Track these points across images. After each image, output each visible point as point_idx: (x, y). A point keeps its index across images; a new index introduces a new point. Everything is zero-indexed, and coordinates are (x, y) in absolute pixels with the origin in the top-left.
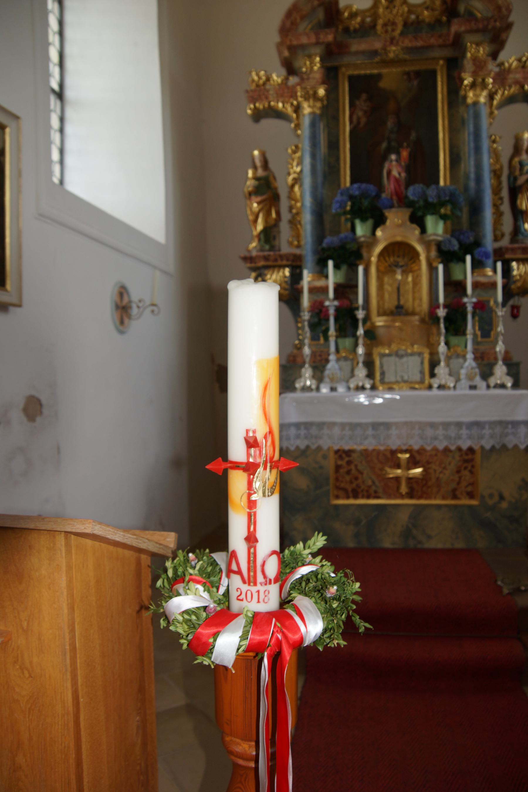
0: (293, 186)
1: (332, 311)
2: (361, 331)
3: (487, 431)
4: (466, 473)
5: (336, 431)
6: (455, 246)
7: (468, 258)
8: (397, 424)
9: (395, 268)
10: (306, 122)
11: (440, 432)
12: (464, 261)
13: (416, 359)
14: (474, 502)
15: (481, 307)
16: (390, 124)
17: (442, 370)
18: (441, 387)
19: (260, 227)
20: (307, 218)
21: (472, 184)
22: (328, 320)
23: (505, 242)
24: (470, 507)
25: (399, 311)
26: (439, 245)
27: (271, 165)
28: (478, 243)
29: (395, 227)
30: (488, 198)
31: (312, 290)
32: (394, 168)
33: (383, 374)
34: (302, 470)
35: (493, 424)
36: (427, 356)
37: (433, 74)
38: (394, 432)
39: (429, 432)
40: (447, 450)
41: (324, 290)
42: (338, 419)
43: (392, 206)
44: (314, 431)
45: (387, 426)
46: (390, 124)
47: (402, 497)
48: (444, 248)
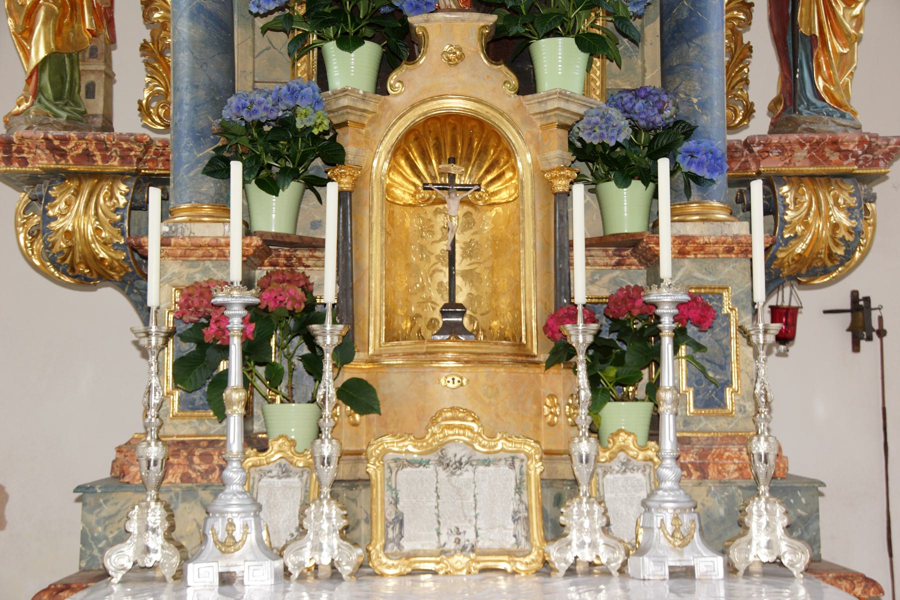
2: (329, 386)
7: (664, 165)
9: (444, 194)
12: (649, 177)
15: (698, 312)
19: (39, 51)
22: (224, 351)
28: (683, 129)
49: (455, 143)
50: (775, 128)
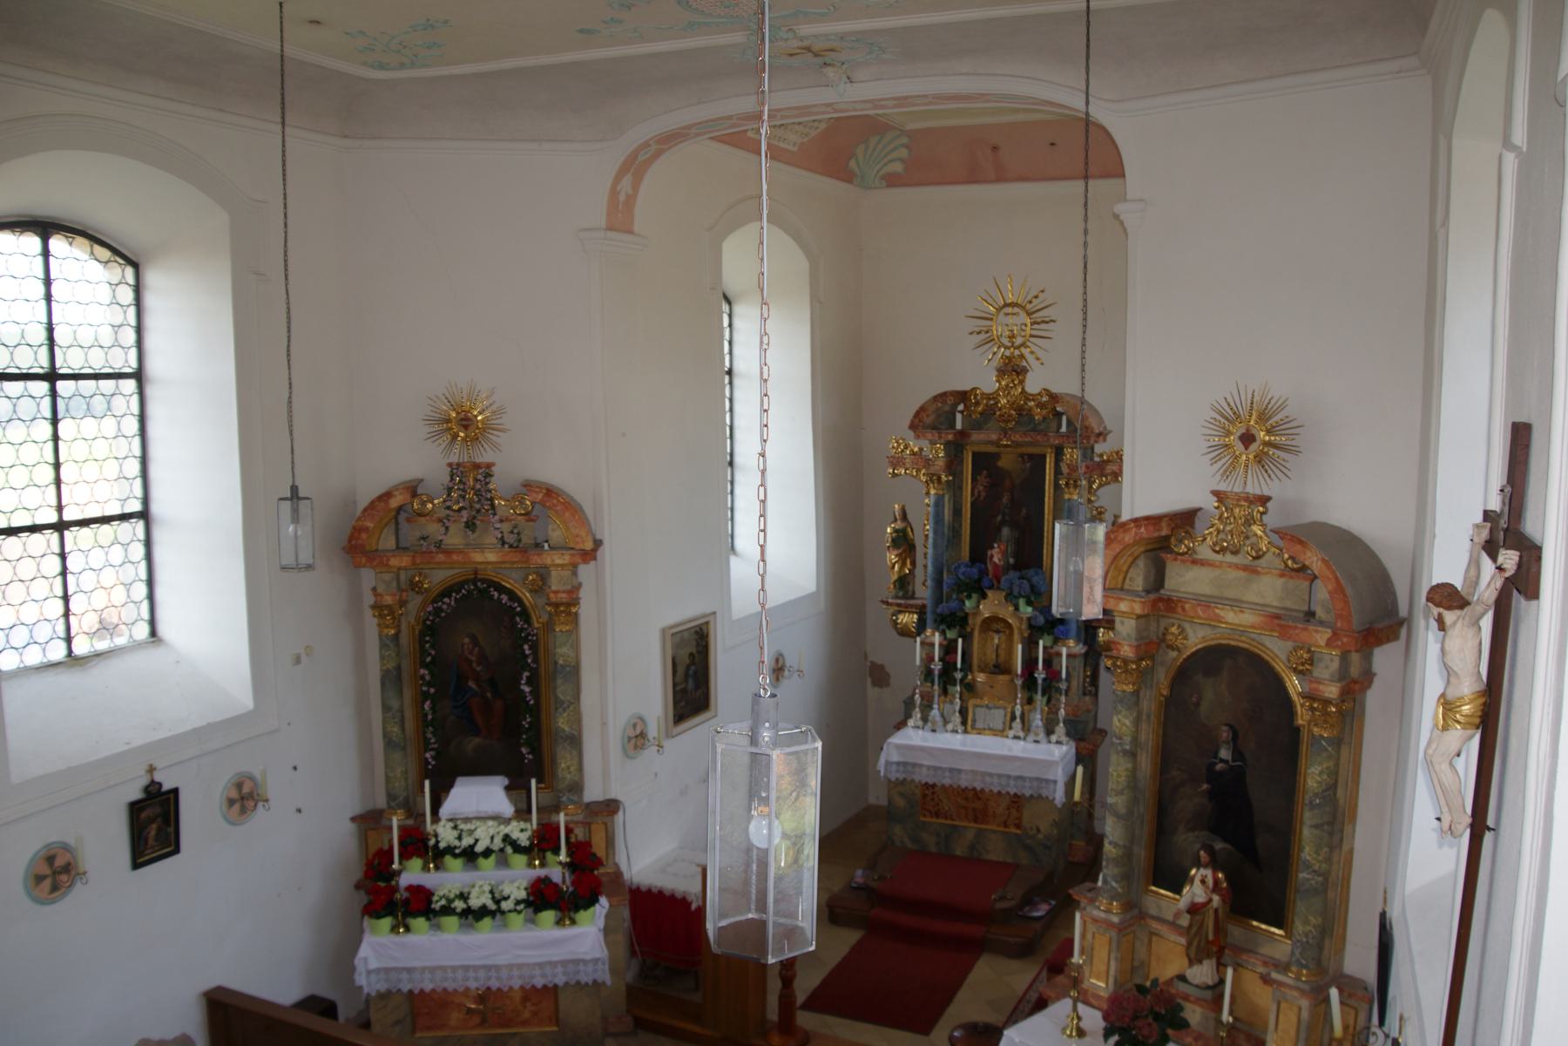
4: (1014, 811)
8: (966, 772)
11: (996, 780)
13: (1002, 712)
16: (1005, 500)
17: (1017, 724)
19: (895, 577)
26: (1029, 619)
27: (909, 517)
32: (996, 556)
33: (974, 721)
34: (902, 795)
35: (1032, 779)
37: (1044, 457)
38: (963, 776)
39: (988, 779)
43: (990, 588)
45: (960, 771)
46: (1005, 500)
49: (993, 624)
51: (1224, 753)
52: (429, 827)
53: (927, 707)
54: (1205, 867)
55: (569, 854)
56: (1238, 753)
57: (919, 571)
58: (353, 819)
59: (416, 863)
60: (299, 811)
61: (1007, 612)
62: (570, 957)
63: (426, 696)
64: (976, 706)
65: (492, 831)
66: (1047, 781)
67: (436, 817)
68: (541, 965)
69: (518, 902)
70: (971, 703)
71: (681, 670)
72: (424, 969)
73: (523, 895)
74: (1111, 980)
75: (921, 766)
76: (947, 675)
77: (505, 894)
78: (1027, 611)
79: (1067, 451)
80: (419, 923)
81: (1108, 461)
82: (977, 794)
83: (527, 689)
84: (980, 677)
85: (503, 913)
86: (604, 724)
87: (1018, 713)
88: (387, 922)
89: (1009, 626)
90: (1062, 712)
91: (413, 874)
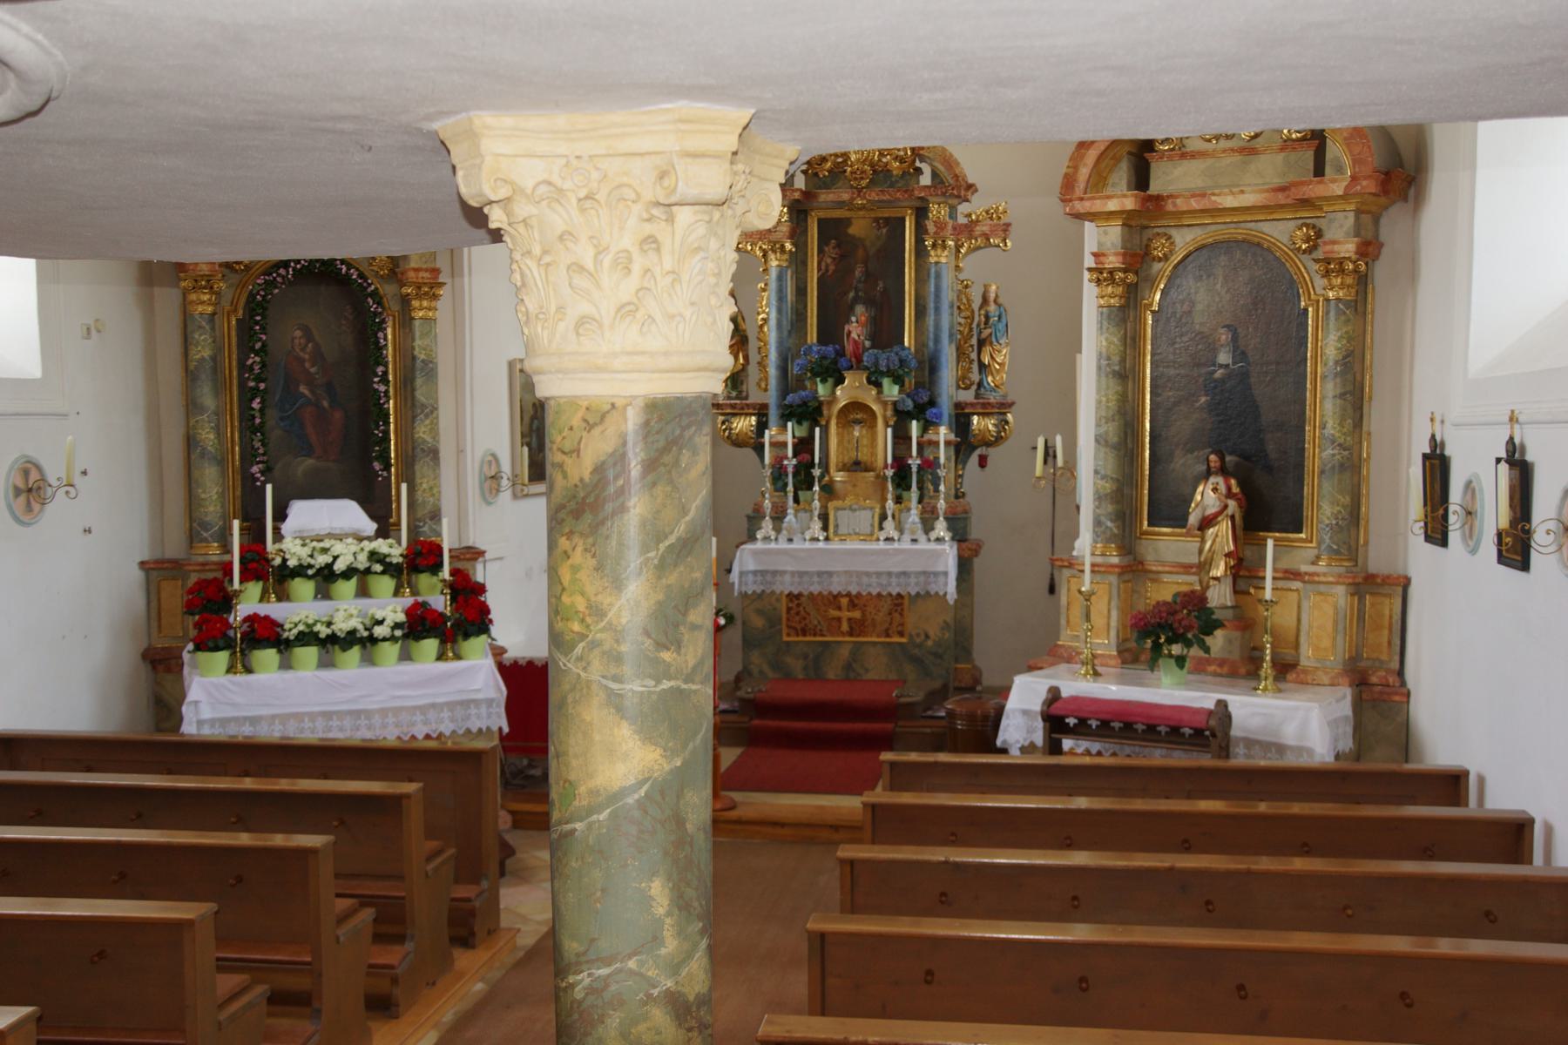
0: (761, 327)
1: (790, 470)
2: (816, 488)
3: (913, 580)
4: (896, 615)
5: (787, 578)
6: (910, 404)
8: (837, 573)
10: (774, 273)
11: (874, 579)
13: (868, 514)
14: (904, 640)
16: (858, 273)
17: (889, 524)
18: (887, 539)
20: (772, 371)
21: (931, 344)
23: (967, 396)
24: (900, 644)
25: (856, 466)
26: (895, 403)
28: (932, 403)
29: (851, 388)
30: (948, 354)
31: (772, 444)
32: (856, 330)
33: (837, 526)
34: (760, 612)
36: (878, 510)
37: (903, 220)
38: (835, 579)
39: (865, 580)
40: (879, 595)
41: (785, 444)
42: (789, 568)
43: (851, 368)
44: (769, 578)
45: (830, 574)
47: (843, 634)
48: (900, 408)
49: (856, 413)
50: (977, 396)
51: (1224, 357)
52: (270, 546)
53: (779, 517)
54: (1216, 474)
55: (452, 574)
56: (1240, 354)
57: (753, 372)
58: (142, 564)
59: (255, 588)
60: (88, 531)
61: (869, 397)
62: (458, 698)
63: (255, 392)
64: (837, 509)
65: (354, 548)
66: (936, 574)
67: (278, 536)
68: (423, 709)
69: (397, 626)
70: (831, 505)
71: (527, 419)
72: (274, 717)
73: (401, 617)
74: (1113, 633)
75: (783, 573)
76: (803, 474)
77: (379, 616)
78: (892, 391)
79: (934, 208)
80: (268, 656)
81: (978, 221)
82: (854, 601)
83: (382, 388)
84: (839, 477)
85: (373, 640)
86: (460, 451)
87: (889, 513)
88: (223, 657)
89: (873, 414)
90: (942, 504)
91: (250, 602)
